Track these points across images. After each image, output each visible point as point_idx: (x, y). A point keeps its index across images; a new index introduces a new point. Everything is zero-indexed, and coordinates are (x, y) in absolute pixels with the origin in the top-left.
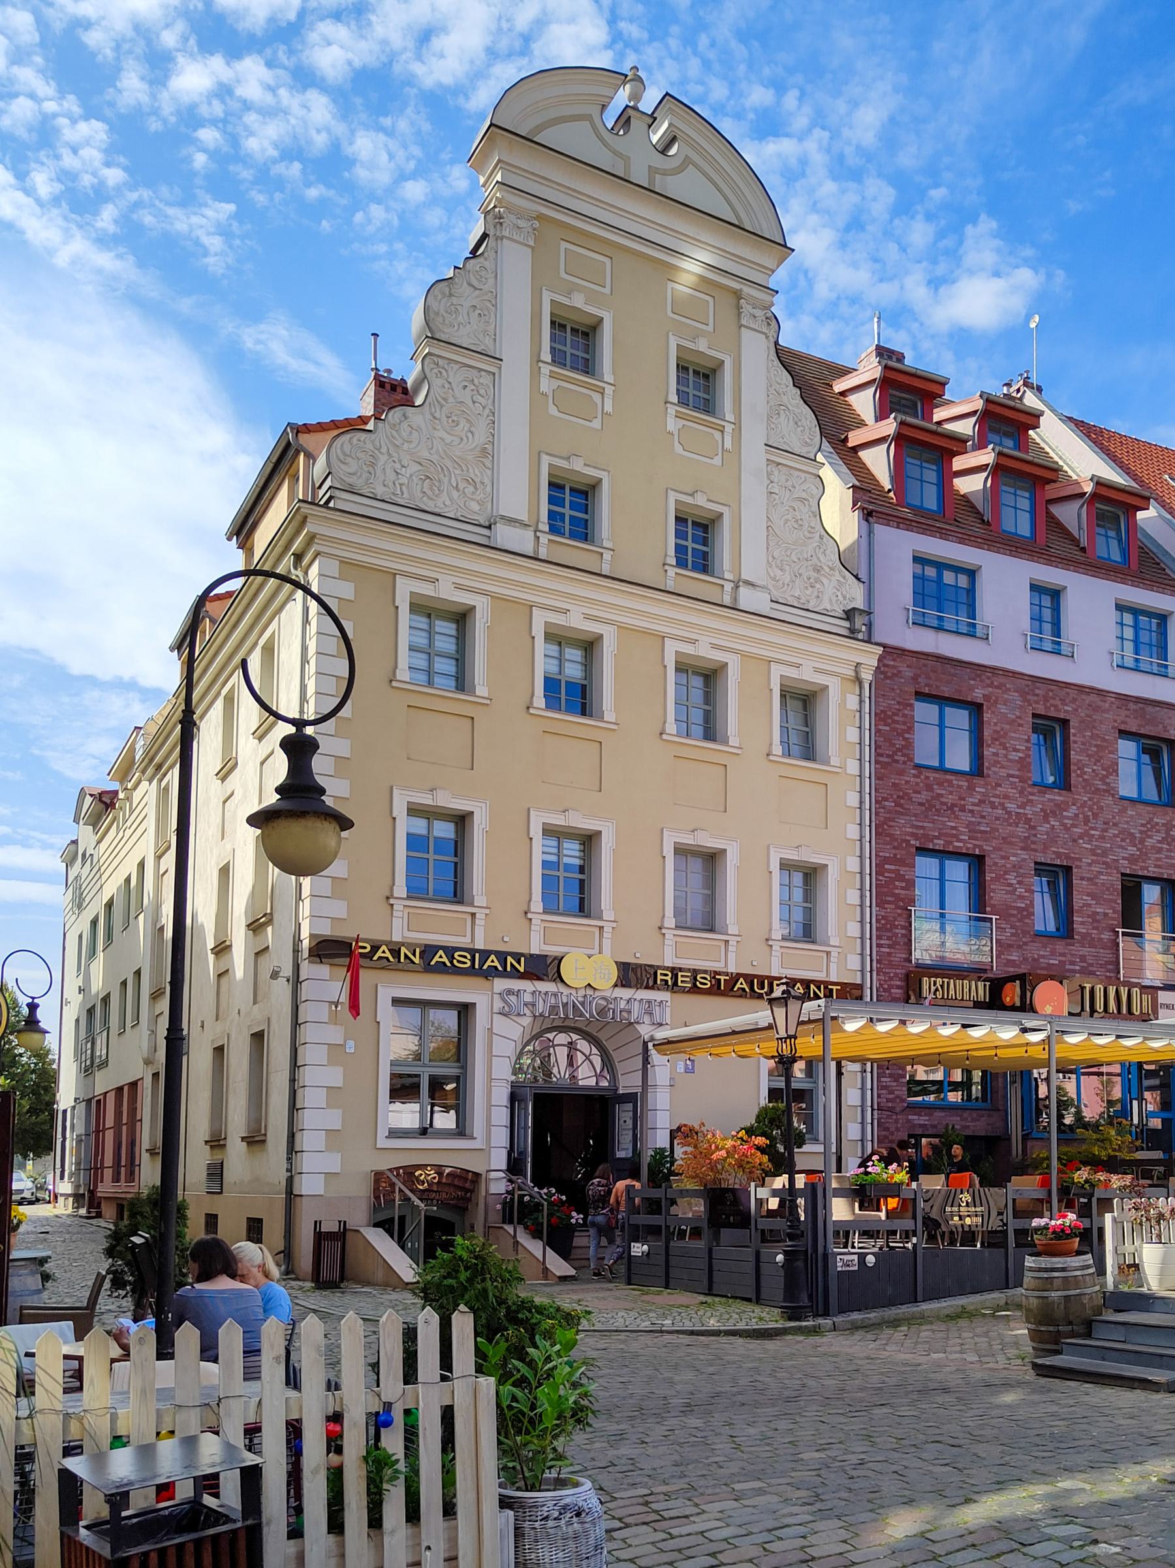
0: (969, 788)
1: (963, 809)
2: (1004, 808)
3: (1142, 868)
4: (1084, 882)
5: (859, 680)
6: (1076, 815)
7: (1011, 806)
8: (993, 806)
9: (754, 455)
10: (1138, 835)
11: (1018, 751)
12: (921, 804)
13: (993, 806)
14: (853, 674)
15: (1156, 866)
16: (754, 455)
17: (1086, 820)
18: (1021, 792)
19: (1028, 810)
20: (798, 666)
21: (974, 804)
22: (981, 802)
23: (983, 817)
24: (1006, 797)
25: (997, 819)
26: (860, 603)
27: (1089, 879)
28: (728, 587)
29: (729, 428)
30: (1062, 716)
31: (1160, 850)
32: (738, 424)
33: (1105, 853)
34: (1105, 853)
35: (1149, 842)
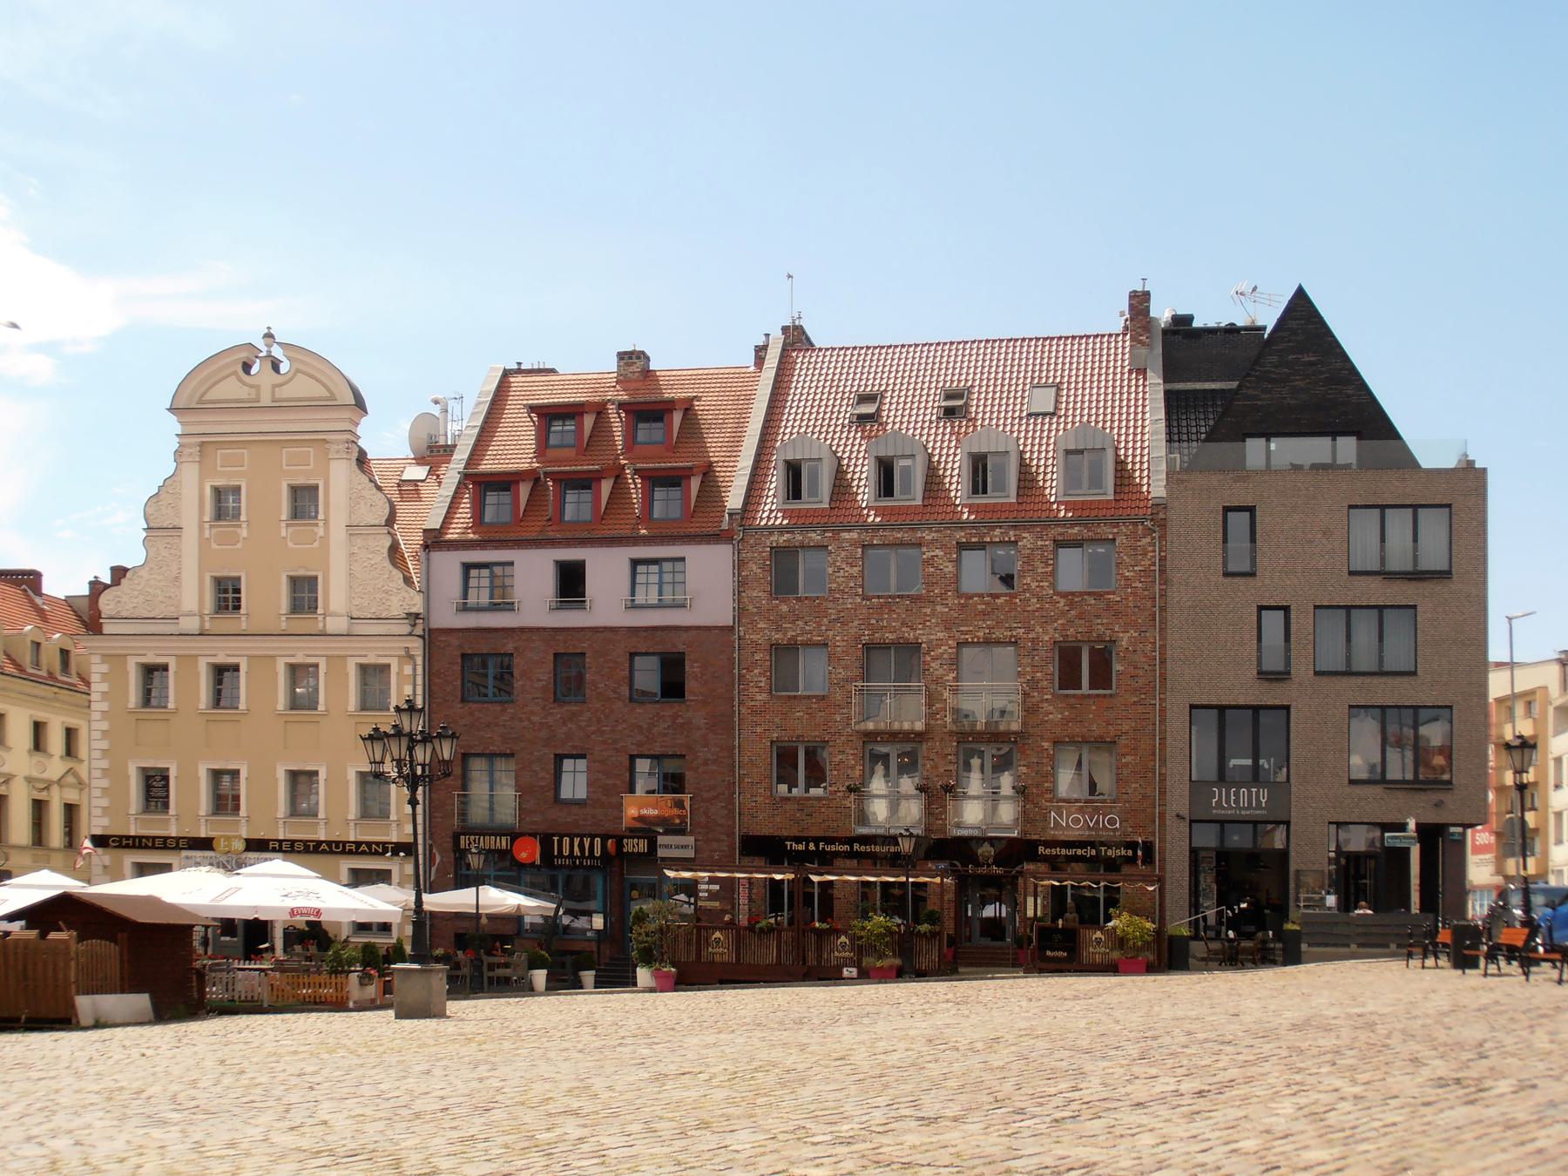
0: (502, 711)
1: (497, 725)
2: (530, 721)
3: (649, 750)
4: (596, 764)
5: (411, 657)
6: (590, 719)
7: (535, 719)
8: (521, 720)
9: (338, 534)
10: (645, 726)
11: (539, 680)
12: (465, 725)
13: (521, 720)
14: (403, 653)
15: (662, 746)
16: (338, 534)
17: (599, 721)
18: (544, 708)
19: (550, 720)
20: (366, 656)
21: (505, 721)
22: (512, 718)
23: (513, 728)
24: (532, 713)
25: (524, 728)
26: (418, 608)
27: (600, 762)
28: (320, 618)
29: (321, 524)
30: (552, 658)
31: (665, 735)
32: (326, 521)
33: (615, 742)
34: (615, 742)
35: (655, 730)
